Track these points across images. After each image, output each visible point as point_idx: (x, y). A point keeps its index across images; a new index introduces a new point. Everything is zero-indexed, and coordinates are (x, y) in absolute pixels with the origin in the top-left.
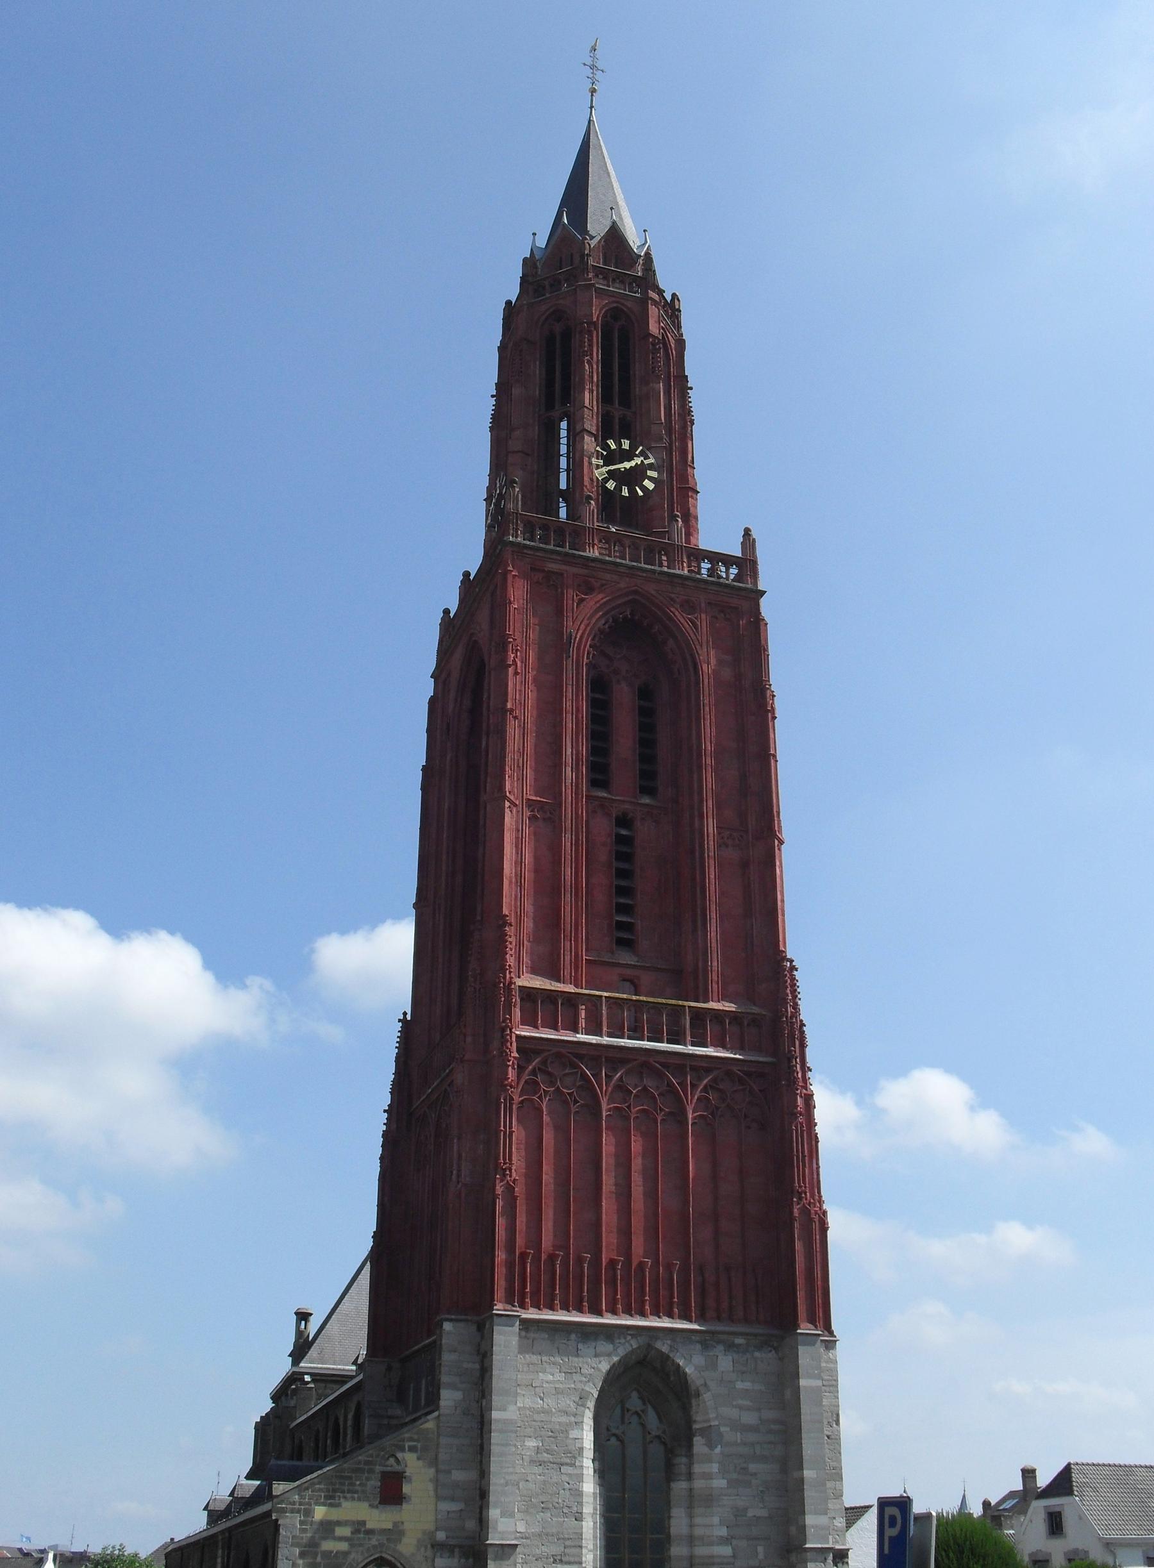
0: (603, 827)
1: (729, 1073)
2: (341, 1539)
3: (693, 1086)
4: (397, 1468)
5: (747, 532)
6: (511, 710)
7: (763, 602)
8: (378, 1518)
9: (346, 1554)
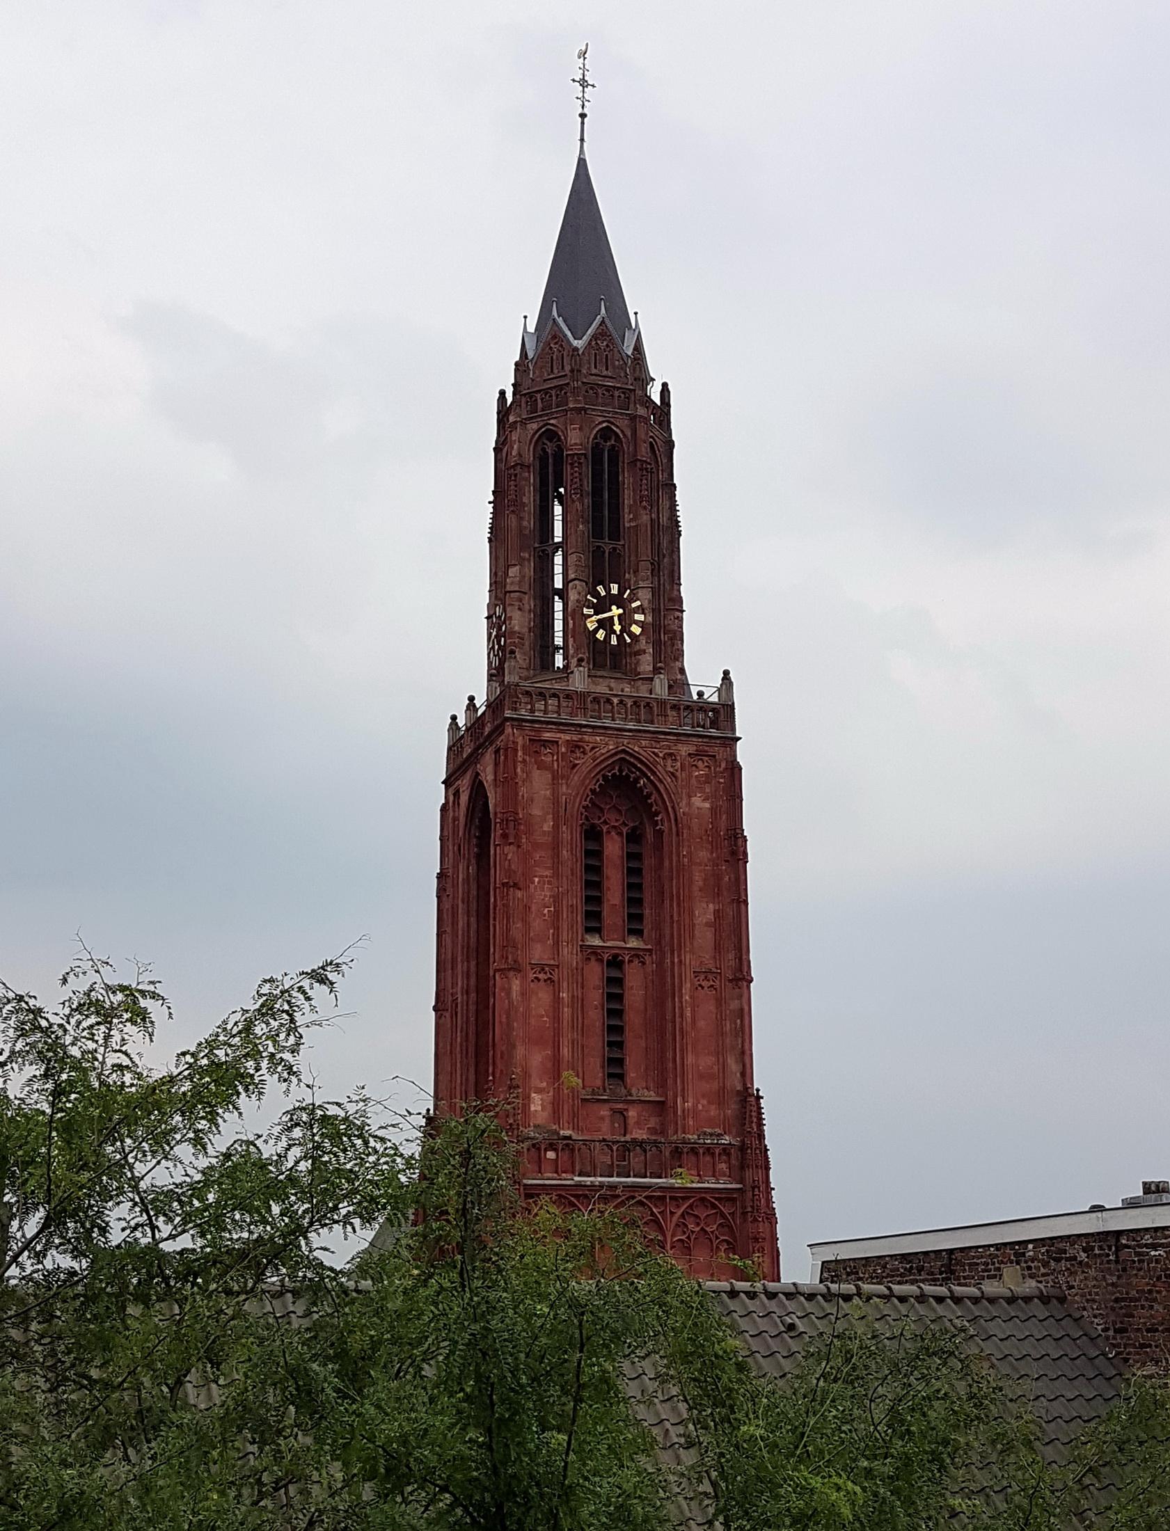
0: (595, 973)
1: (703, 1200)
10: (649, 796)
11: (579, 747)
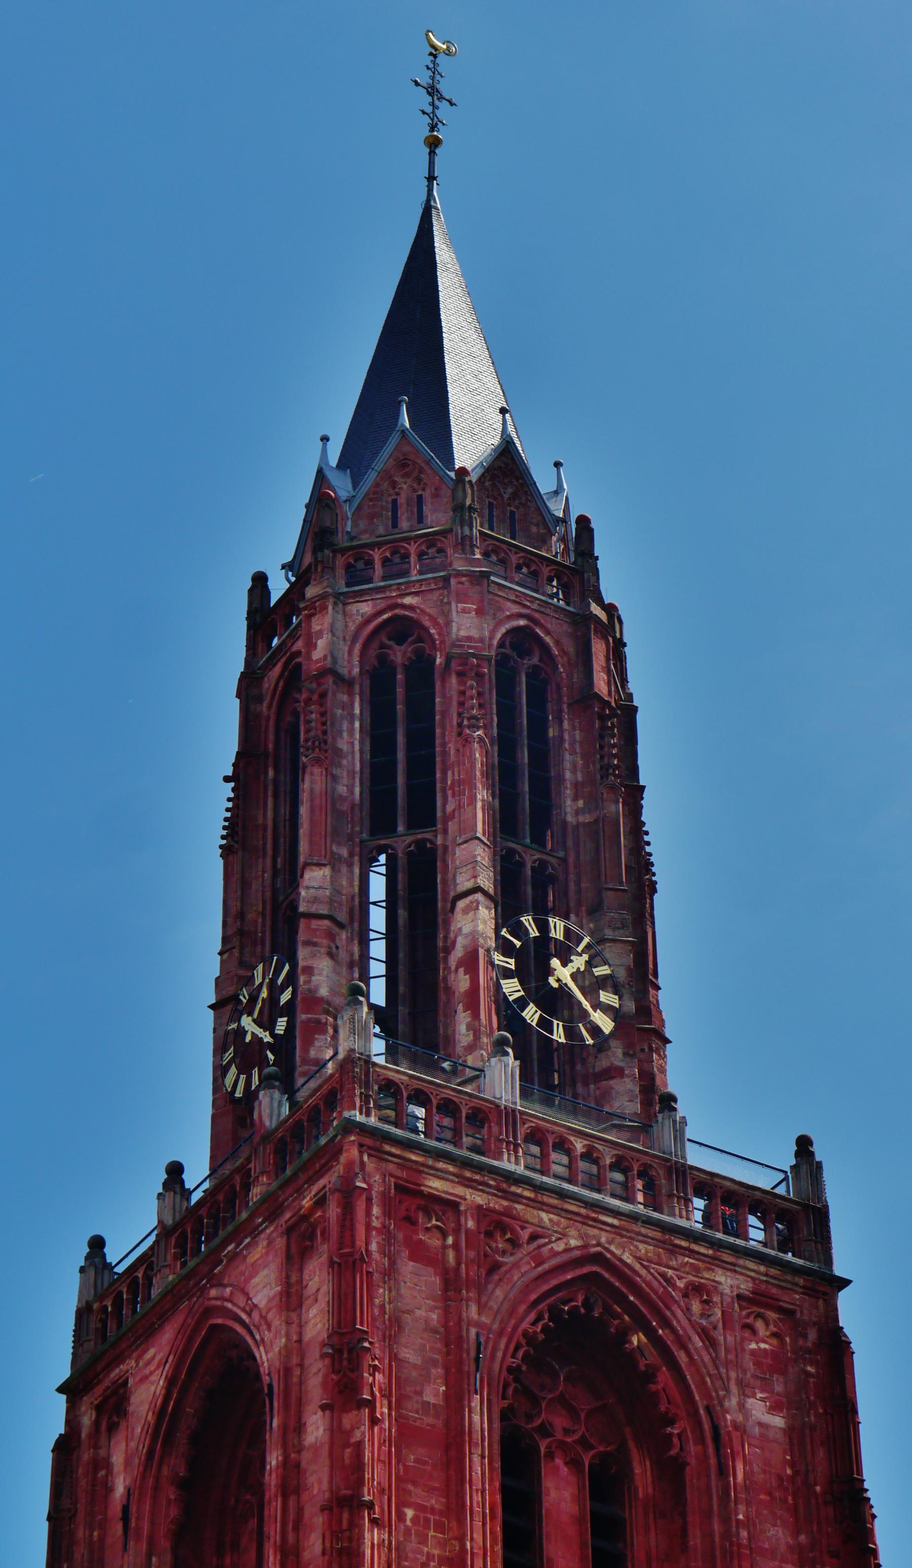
5: (804, 1145)
6: (370, 1506)
7: (847, 1305)
10: (650, 1375)
11: (502, 1228)
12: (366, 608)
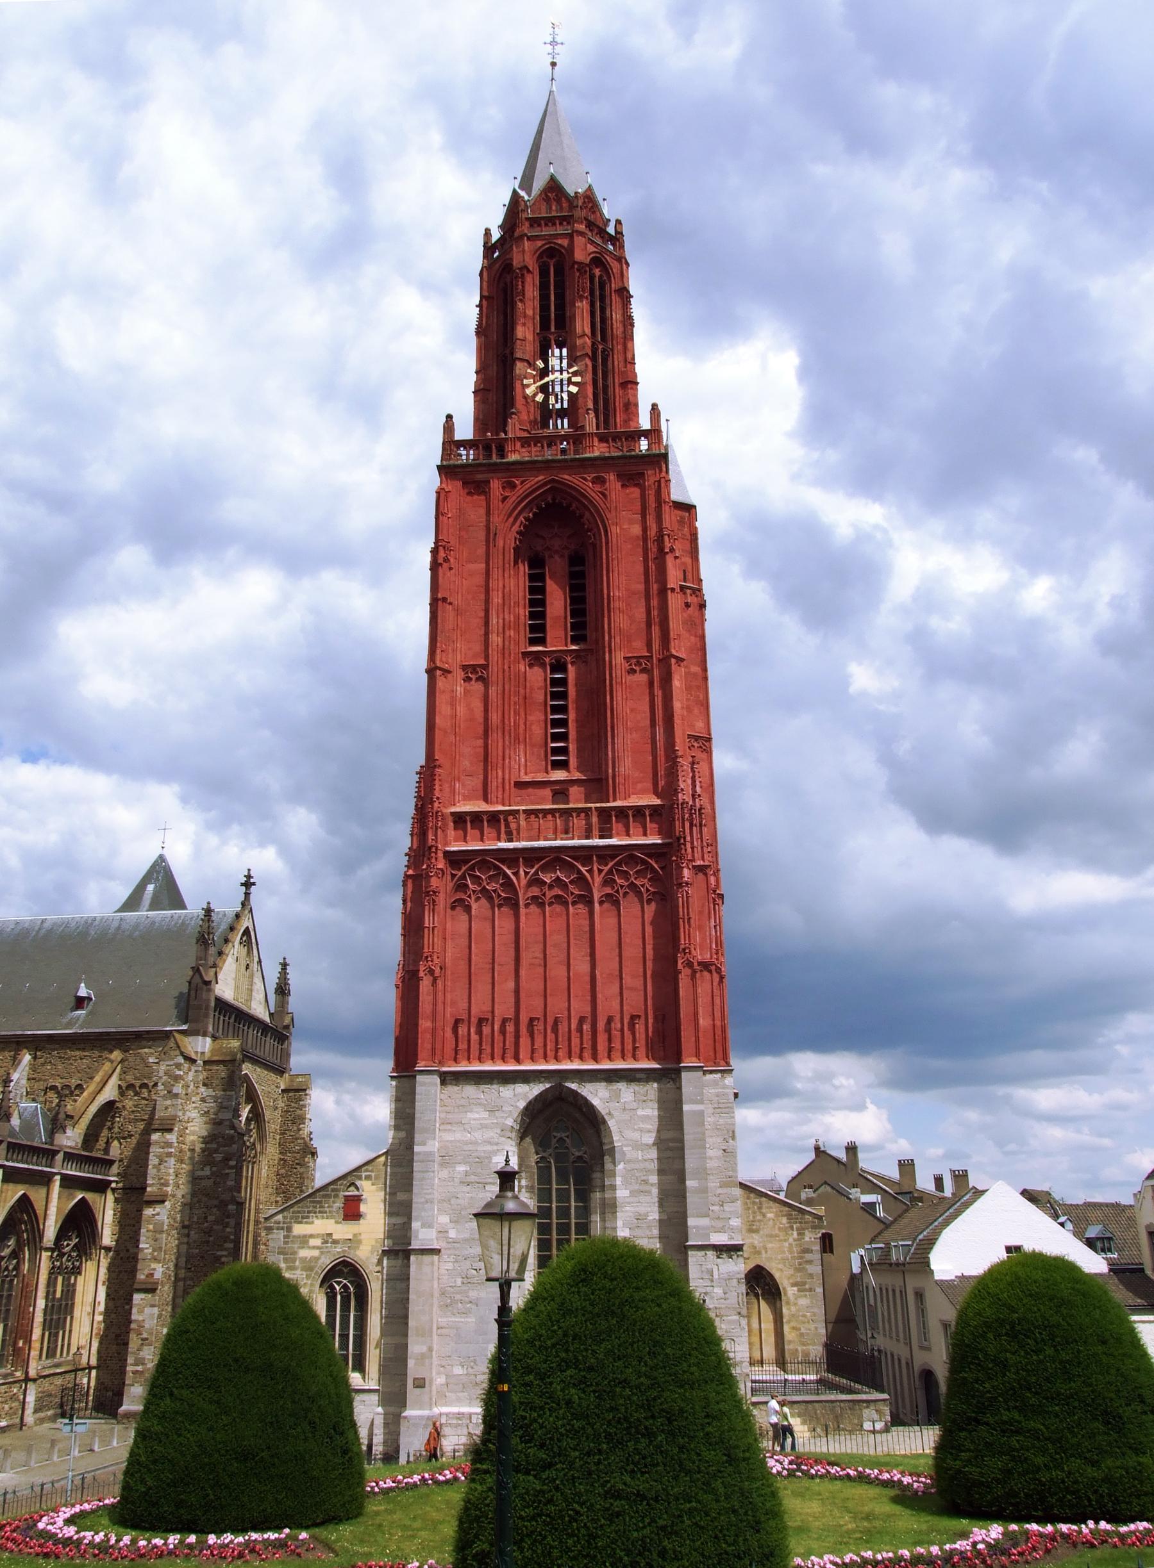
0: (537, 677)
2: (314, 1247)
3: (600, 871)
4: (356, 1193)
8: (342, 1230)
9: (317, 1259)
12: (497, 266)
